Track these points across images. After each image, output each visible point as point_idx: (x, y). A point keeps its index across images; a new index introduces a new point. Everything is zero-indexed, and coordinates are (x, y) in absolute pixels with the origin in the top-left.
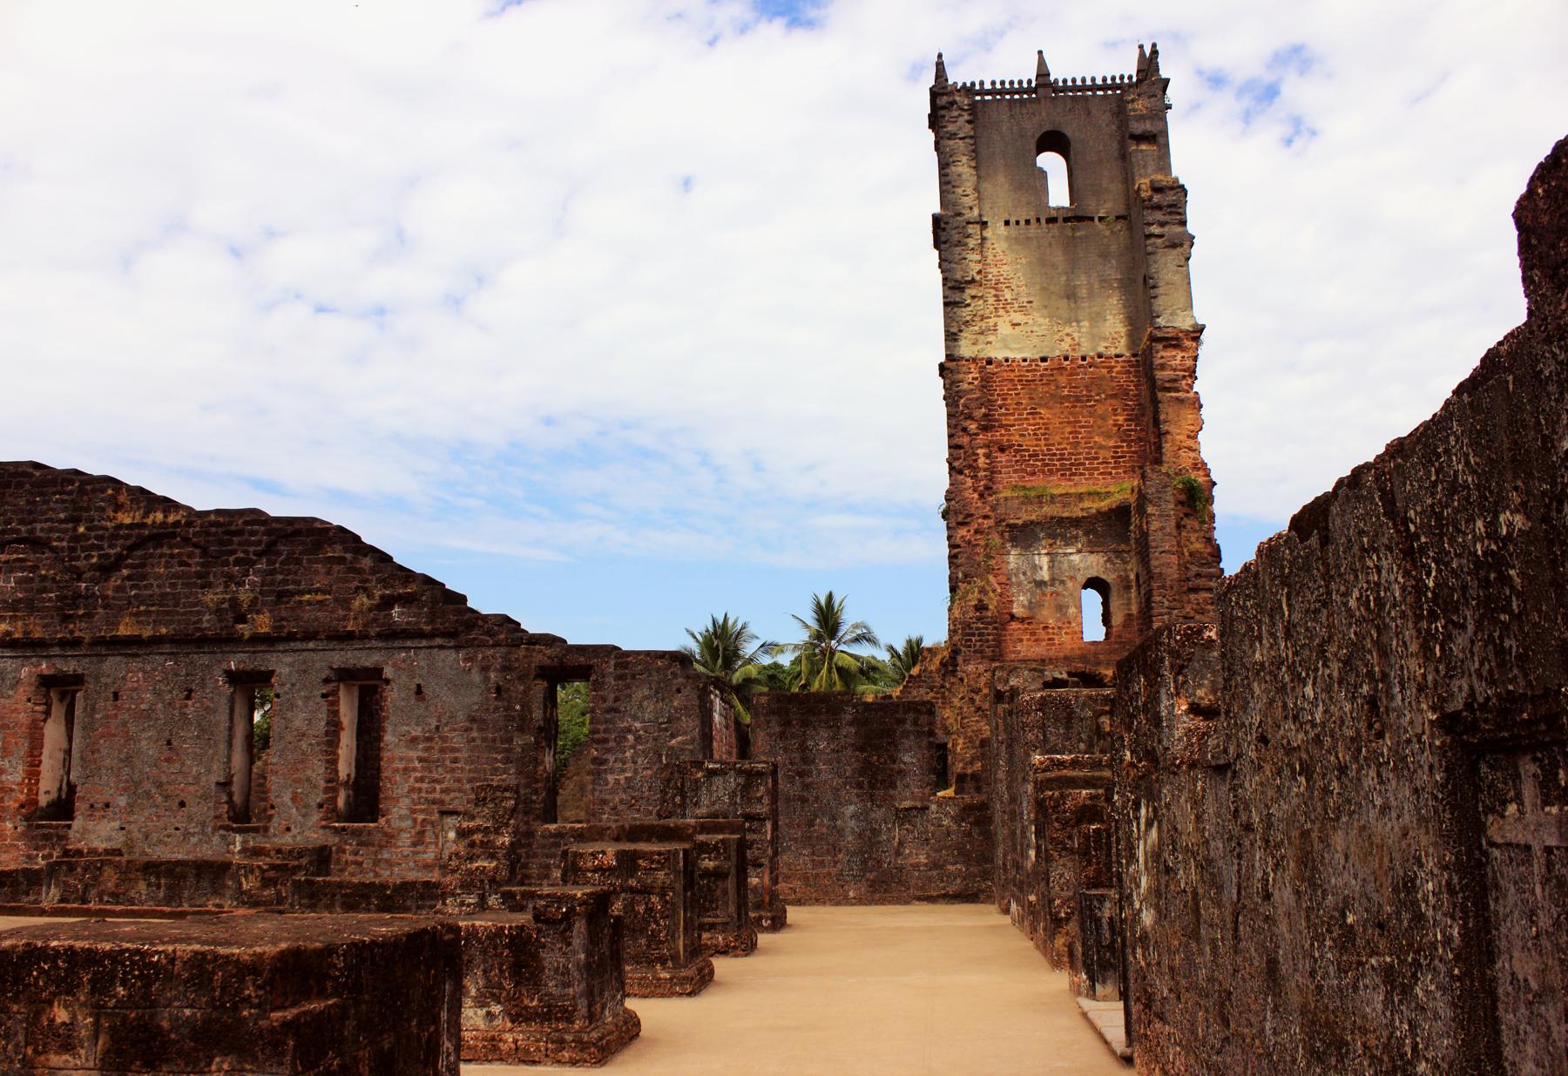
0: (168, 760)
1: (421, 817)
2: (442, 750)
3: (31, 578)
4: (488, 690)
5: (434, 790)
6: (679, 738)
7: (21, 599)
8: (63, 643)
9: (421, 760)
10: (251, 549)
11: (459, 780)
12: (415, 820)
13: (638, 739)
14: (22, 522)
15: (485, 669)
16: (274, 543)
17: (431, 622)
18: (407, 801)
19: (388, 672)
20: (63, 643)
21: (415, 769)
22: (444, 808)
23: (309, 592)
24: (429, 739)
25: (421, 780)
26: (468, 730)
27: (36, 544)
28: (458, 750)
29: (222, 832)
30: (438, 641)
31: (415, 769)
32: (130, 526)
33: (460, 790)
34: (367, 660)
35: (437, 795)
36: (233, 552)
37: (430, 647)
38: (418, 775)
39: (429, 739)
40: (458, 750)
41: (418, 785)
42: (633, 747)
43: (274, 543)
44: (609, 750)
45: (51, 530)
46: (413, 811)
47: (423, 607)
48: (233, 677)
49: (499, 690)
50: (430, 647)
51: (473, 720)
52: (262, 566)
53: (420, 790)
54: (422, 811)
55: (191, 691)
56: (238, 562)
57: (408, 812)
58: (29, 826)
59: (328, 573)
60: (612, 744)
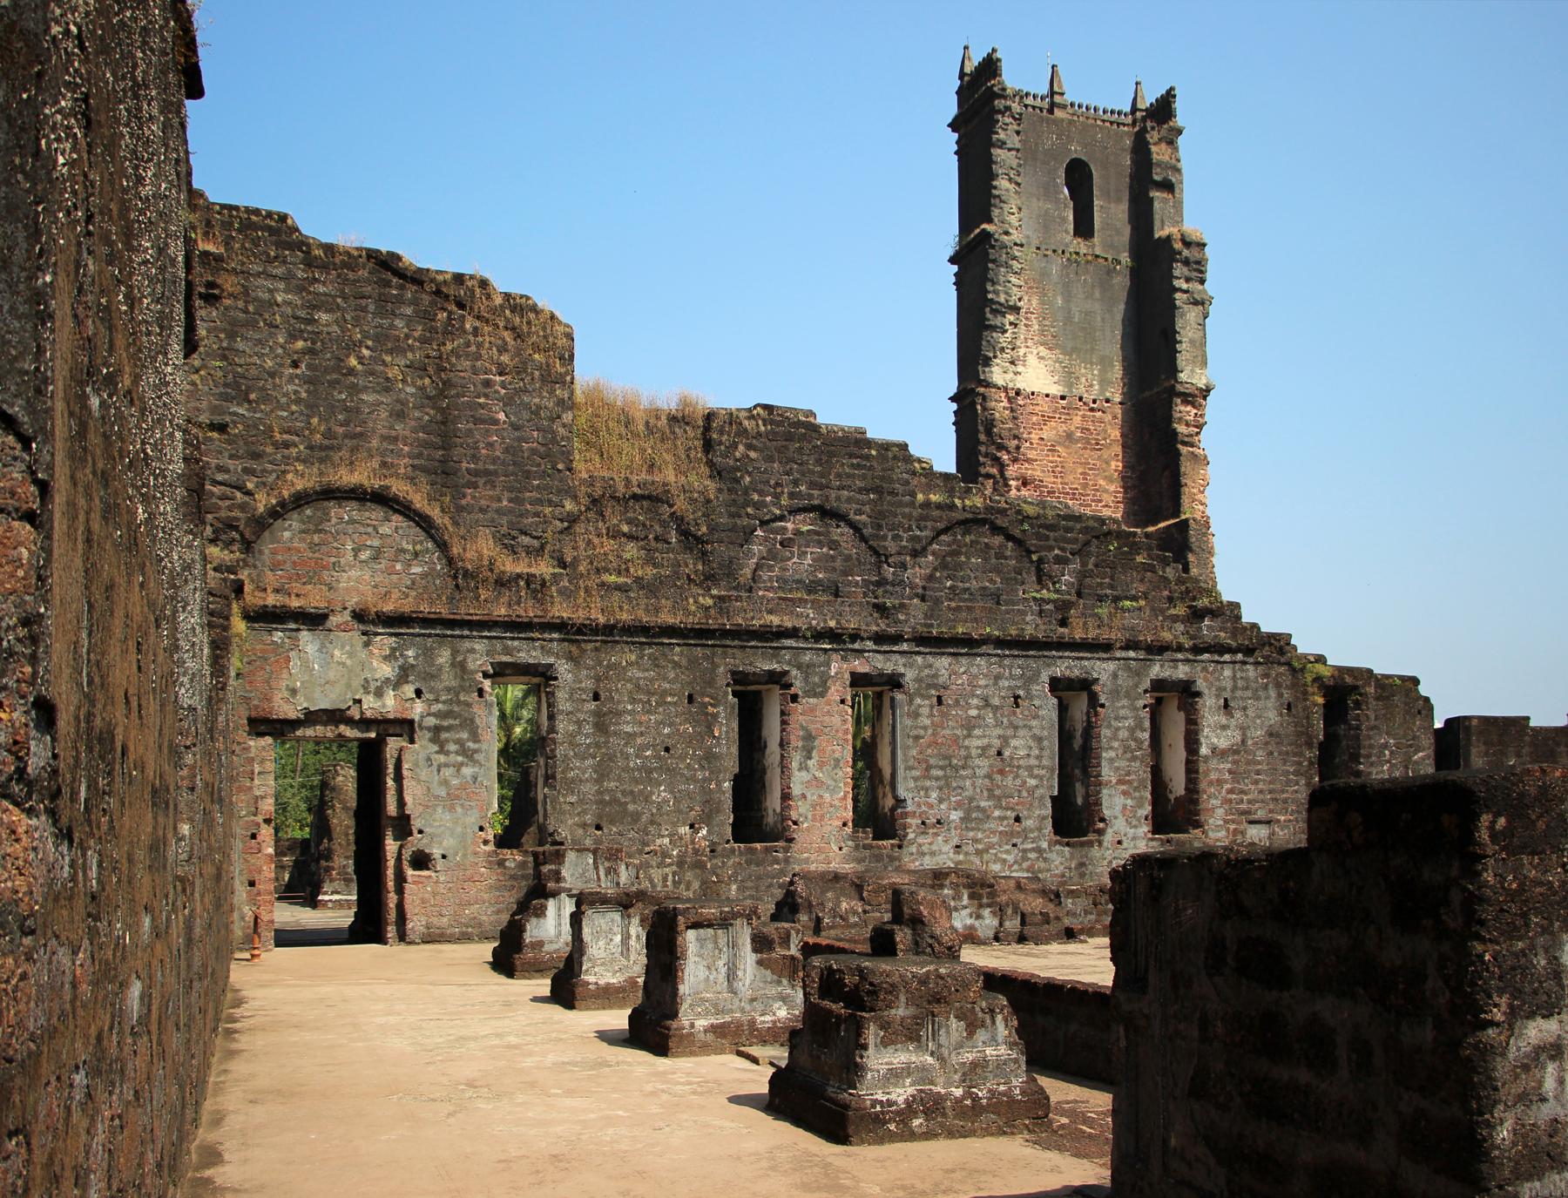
0: (1001, 772)
1: (1232, 827)
2: (1248, 763)
3: (832, 557)
4: (1282, 705)
5: (1242, 801)
6: (1420, 754)
7: (820, 580)
8: (879, 638)
9: (1230, 772)
10: (1069, 546)
11: (1261, 792)
12: (1228, 830)
13: (1392, 753)
14: (812, 485)
15: (1278, 685)
16: (1087, 543)
17: (1234, 636)
18: (1220, 812)
19: (1201, 685)
20: (879, 638)
21: (1226, 781)
22: (1252, 817)
23: (1127, 598)
24: (1236, 752)
25: (1230, 791)
26: (1267, 743)
27: (826, 513)
28: (1259, 763)
29: (1058, 847)
30: (1240, 656)
31: (1226, 781)
32: (939, 506)
33: (1263, 801)
34: (1182, 672)
35: (1244, 806)
36: (1051, 549)
37: (1234, 662)
38: (1229, 786)
39: (1236, 752)
40: (1259, 763)
41: (1230, 796)
42: (1389, 761)
43: (1087, 543)
44: (1372, 764)
45: (849, 500)
46: (1227, 822)
47: (1227, 621)
48: (1056, 685)
49: (1289, 707)
50: (1234, 662)
51: (1271, 735)
52: (1076, 565)
53: (1230, 801)
54: (1233, 821)
55: (1017, 697)
56: (1059, 560)
57: (1221, 823)
58: (857, 847)
59: (1142, 581)
60: (1373, 759)
